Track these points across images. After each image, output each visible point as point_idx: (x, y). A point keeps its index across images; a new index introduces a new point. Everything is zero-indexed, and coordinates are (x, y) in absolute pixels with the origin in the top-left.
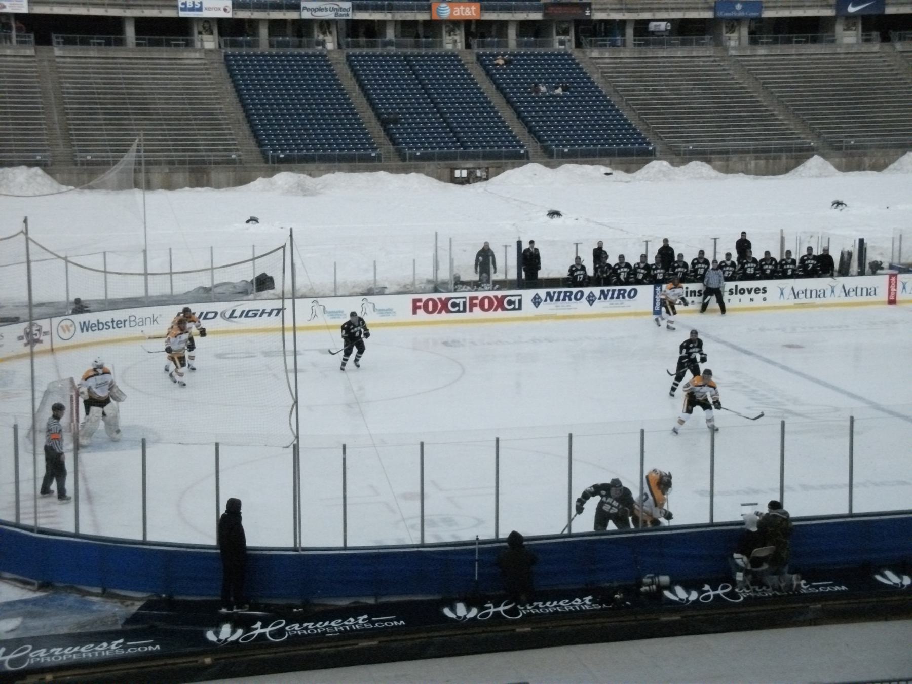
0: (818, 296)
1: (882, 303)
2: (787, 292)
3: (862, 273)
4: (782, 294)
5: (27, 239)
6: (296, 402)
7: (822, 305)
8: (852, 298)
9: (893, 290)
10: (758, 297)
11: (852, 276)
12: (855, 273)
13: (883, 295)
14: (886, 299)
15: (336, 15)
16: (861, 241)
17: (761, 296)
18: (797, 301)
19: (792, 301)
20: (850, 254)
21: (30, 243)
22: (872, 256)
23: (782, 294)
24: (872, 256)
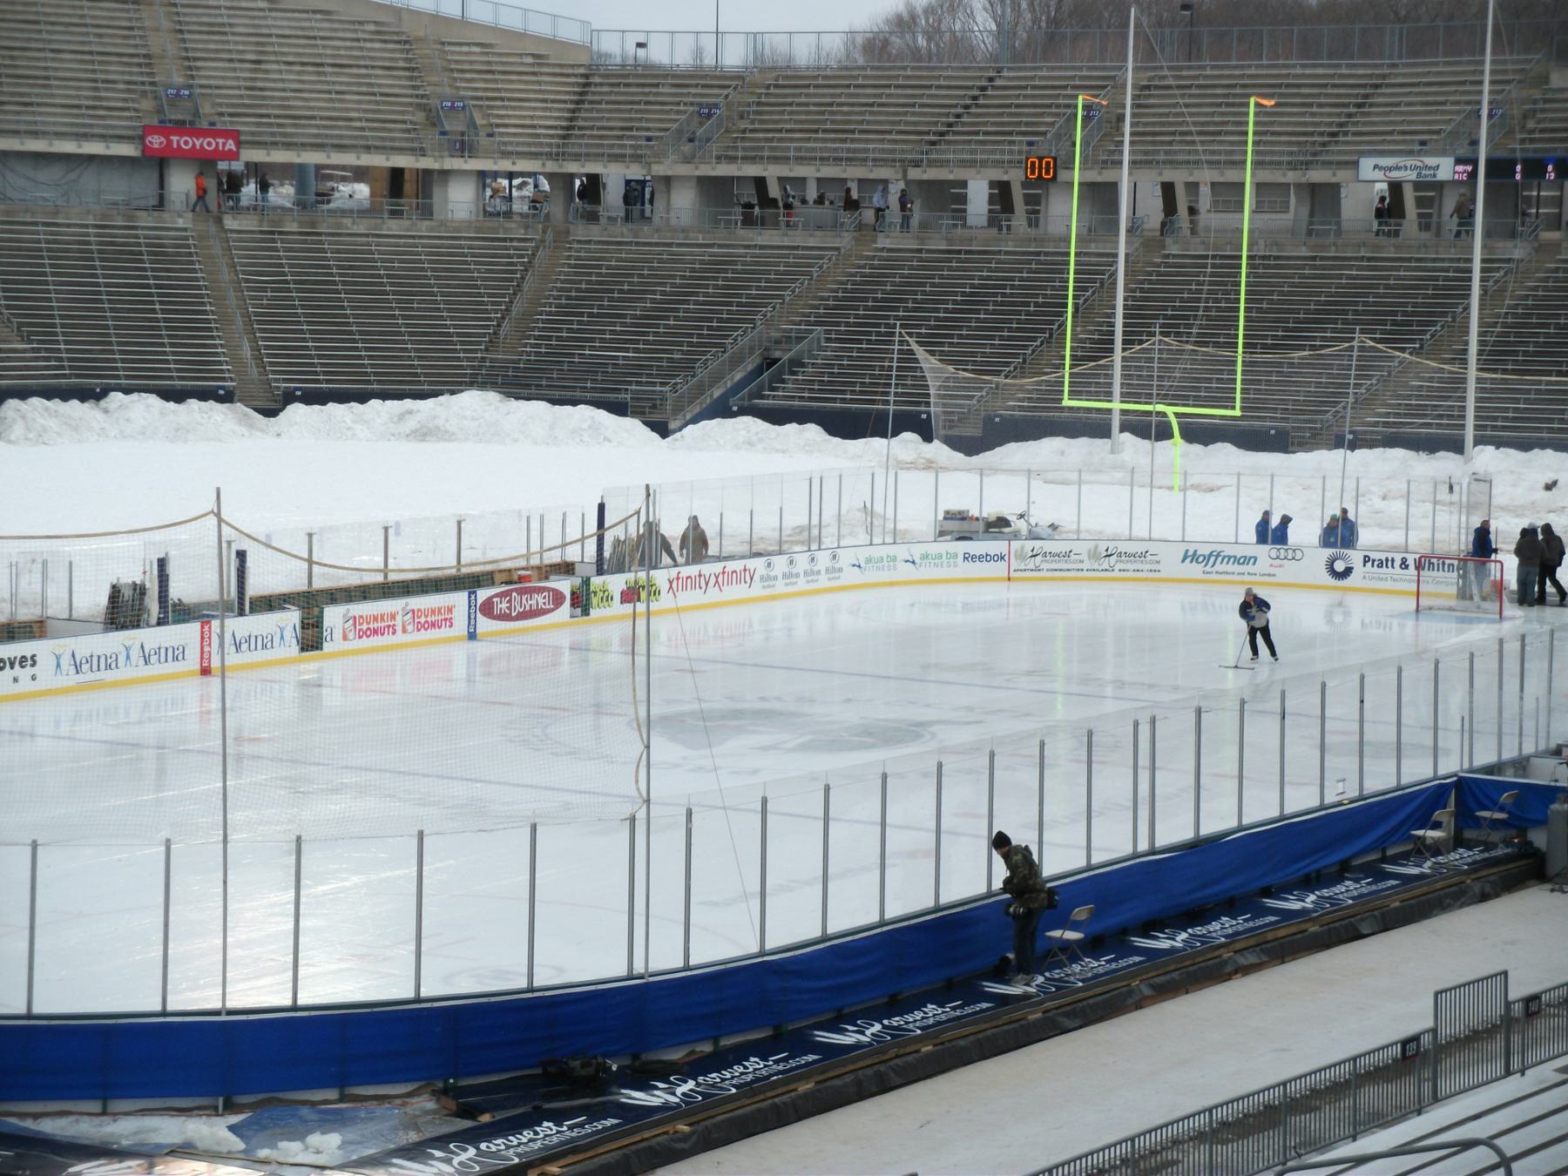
0: (108, 667)
1: (189, 674)
2: (66, 661)
3: (161, 622)
4: (58, 665)
5: (220, 520)
6: (648, 747)
7: (116, 685)
8: (156, 669)
9: (206, 649)
10: (24, 674)
11: (149, 626)
12: (154, 620)
13: (192, 662)
14: (198, 667)
15: (1419, 175)
16: (162, 563)
17: (29, 671)
18: (81, 678)
19: (73, 679)
20: (140, 590)
21: (224, 526)
22: (179, 590)
23: (58, 665)
24: (179, 590)
